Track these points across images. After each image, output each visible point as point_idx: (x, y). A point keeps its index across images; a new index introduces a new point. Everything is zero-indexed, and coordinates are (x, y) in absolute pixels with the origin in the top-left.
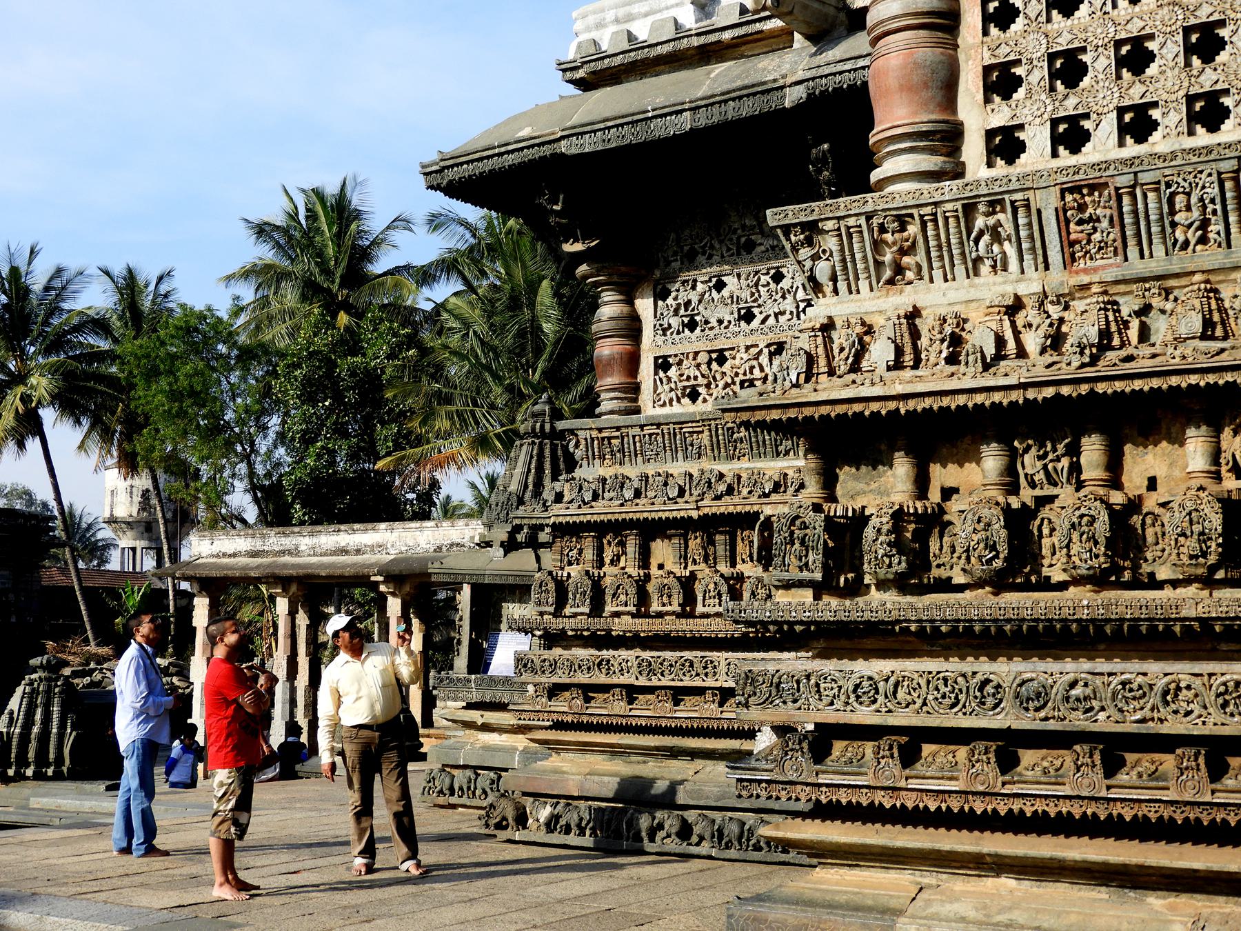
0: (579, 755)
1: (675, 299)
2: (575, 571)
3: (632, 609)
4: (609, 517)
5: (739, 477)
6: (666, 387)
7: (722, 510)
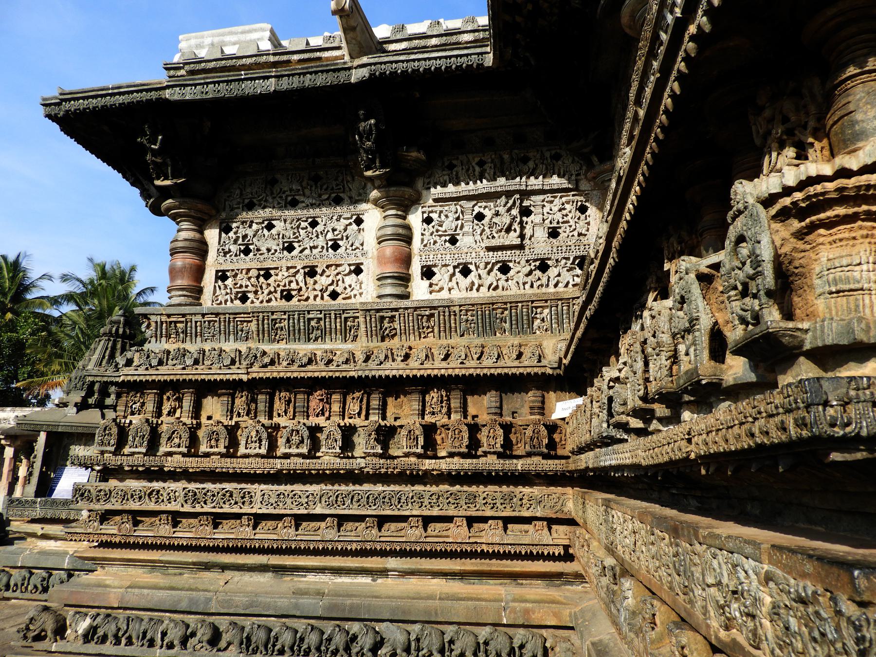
0: (122, 568)
1: (236, 233)
2: (136, 420)
3: (184, 450)
4: (172, 377)
5: (279, 355)
6: (223, 292)
7: (268, 375)
